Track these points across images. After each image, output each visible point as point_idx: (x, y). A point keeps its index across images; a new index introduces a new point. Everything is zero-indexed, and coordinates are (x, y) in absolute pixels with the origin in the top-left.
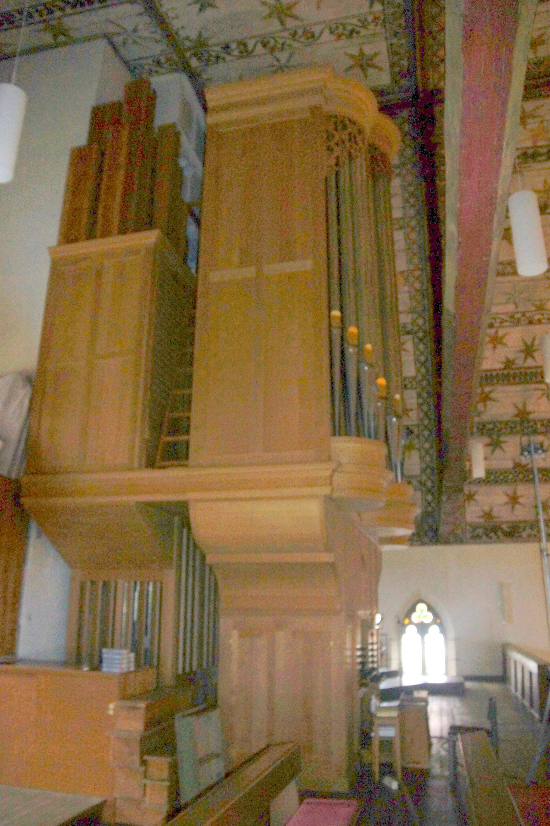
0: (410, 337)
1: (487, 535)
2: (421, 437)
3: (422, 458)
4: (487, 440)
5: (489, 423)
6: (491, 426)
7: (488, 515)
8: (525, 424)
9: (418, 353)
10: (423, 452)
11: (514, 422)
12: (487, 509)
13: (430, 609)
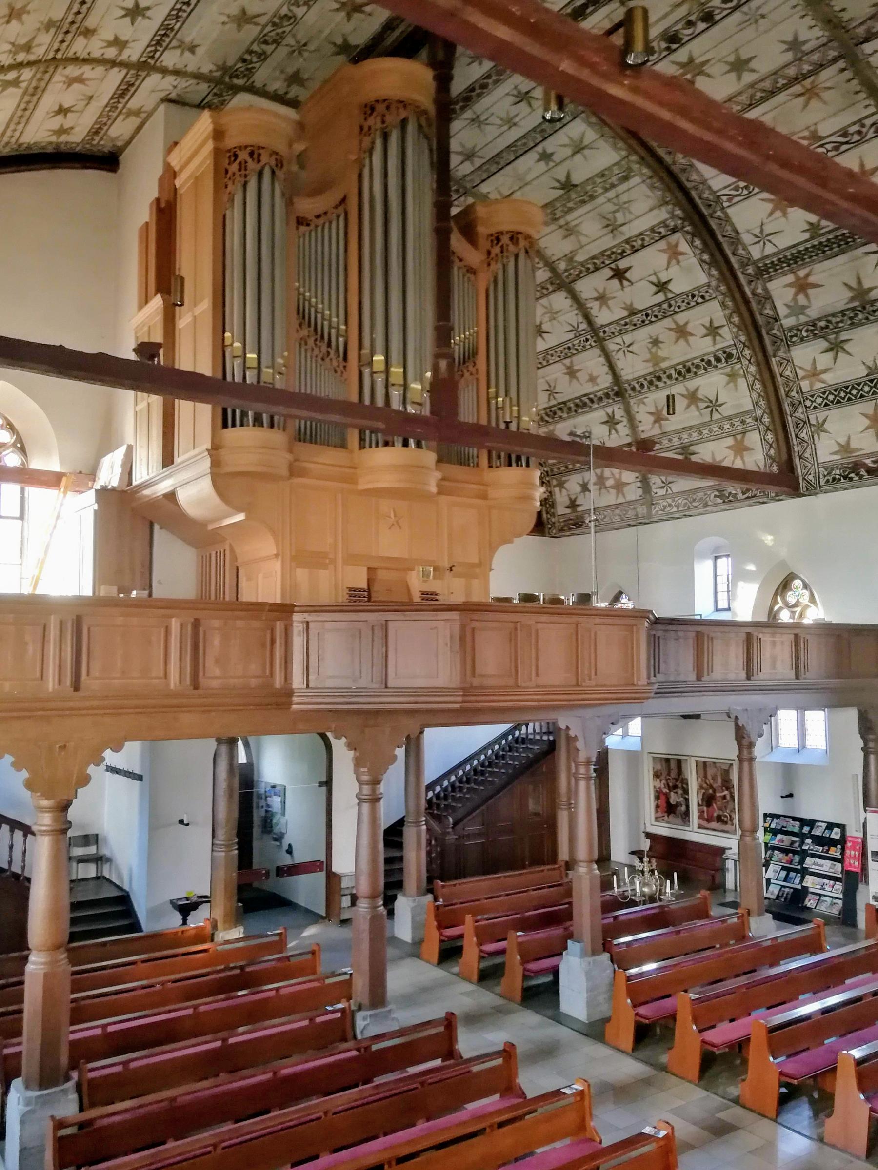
0: (678, 235)
1: (845, 478)
3: (751, 388)
4: (823, 344)
5: (819, 319)
6: (823, 324)
7: (845, 448)
8: (869, 308)
9: (698, 252)
10: (751, 379)
11: (853, 309)
12: (842, 440)
13: (806, 586)
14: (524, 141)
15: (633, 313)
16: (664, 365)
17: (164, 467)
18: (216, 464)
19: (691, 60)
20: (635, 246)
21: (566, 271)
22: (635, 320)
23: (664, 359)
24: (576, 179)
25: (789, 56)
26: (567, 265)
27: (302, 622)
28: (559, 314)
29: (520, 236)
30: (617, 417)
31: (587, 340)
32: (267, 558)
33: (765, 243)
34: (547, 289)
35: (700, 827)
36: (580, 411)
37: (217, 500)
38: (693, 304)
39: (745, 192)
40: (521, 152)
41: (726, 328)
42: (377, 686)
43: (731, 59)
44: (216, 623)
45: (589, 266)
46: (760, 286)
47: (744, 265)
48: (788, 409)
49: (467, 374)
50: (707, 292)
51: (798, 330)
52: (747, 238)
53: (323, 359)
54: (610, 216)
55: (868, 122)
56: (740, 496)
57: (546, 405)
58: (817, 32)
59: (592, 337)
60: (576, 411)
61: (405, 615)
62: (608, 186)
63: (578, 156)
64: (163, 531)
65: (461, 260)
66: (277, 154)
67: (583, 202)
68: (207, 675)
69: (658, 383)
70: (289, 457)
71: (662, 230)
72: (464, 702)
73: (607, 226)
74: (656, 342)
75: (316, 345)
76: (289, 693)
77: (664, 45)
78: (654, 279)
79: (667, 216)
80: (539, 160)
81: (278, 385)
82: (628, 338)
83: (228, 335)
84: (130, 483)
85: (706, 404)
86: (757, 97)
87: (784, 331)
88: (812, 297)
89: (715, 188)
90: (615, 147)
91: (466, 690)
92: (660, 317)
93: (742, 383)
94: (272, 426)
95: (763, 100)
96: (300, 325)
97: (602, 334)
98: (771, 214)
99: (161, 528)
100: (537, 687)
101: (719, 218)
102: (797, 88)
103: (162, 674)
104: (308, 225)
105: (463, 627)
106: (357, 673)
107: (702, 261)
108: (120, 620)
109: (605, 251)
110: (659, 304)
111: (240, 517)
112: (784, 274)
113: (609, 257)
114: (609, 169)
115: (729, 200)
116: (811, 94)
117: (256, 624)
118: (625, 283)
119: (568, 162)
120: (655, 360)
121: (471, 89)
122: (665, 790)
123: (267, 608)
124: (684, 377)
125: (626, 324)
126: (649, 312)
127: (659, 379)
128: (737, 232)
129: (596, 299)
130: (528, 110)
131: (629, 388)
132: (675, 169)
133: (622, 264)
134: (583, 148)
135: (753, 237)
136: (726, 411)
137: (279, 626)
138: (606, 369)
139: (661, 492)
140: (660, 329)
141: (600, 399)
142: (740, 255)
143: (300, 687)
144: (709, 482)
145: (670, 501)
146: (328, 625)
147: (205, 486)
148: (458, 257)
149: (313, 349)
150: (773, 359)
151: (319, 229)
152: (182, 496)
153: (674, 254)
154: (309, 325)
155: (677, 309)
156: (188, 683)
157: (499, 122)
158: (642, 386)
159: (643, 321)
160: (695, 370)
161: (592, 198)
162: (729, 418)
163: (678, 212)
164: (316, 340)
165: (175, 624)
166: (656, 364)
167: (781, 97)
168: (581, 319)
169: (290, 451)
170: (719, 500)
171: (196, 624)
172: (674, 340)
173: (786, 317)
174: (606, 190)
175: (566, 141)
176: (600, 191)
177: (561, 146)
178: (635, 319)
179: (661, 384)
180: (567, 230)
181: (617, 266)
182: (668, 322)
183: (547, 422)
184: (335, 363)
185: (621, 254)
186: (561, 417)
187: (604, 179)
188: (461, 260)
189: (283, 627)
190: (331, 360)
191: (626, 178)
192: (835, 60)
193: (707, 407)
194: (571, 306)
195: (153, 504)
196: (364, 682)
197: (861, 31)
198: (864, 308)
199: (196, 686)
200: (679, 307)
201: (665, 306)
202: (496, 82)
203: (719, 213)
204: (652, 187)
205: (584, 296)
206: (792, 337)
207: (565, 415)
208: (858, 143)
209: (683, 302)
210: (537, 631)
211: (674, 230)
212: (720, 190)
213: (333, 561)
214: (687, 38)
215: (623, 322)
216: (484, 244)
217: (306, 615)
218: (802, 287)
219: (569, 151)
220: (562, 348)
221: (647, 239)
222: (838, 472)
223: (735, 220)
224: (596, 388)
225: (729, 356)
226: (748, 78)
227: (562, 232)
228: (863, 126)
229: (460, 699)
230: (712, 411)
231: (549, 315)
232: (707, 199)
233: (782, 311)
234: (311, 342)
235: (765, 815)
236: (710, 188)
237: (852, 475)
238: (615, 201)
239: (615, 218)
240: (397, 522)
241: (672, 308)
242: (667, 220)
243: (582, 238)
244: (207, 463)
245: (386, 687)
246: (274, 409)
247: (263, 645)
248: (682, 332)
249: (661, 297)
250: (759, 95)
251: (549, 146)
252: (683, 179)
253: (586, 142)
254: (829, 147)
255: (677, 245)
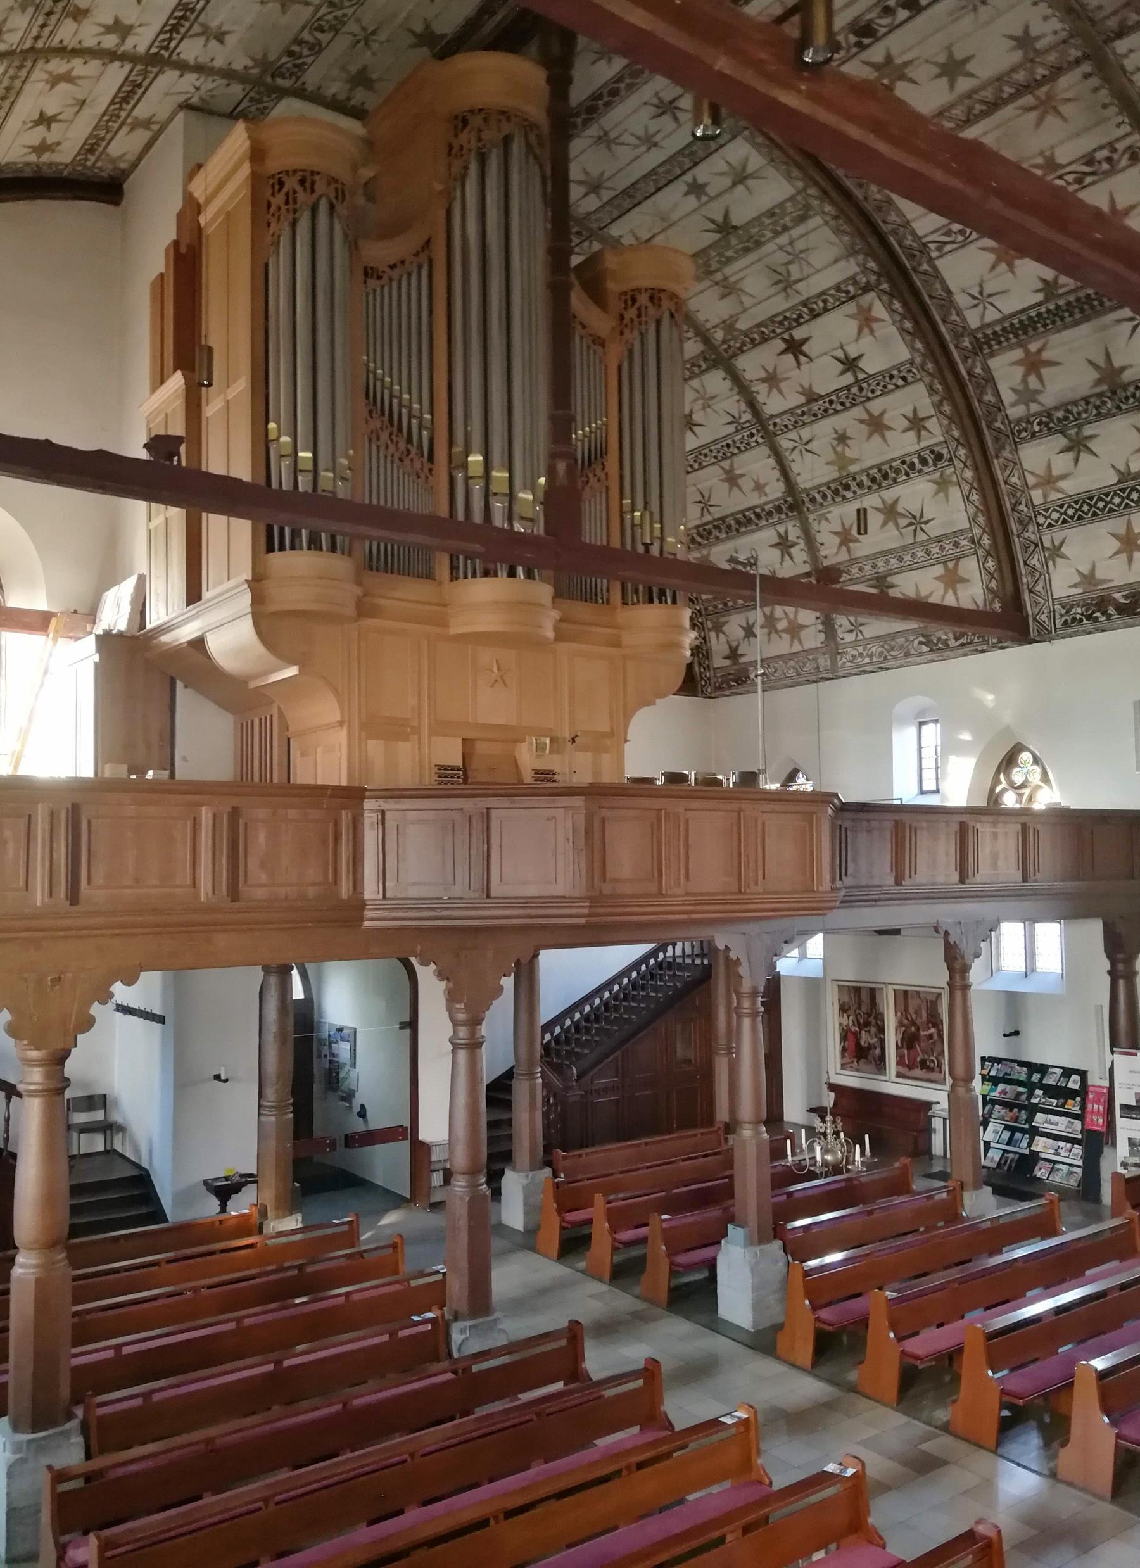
0: (872, 294)
1: (1089, 617)
2: (956, 462)
3: (967, 499)
4: (1060, 441)
5: (1056, 408)
7: (1089, 579)
8: (1121, 394)
9: (898, 318)
10: (966, 488)
11: (1100, 395)
12: (1085, 570)
13: (1036, 760)
14: (668, 166)
15: (812, 397)
16: (853, 469)
17: (188, 604)
18: (258, 600)
19: (889, 59)
20: (815, 309)
21: (724, 342)
22: (816, 408)
23: (854, 461)
24: (737, 219)
25: (1017, 56)
26: (725, 335)
27: (377, 811)
28: (715, 401)
29: (663, 295)
30: (792, 537)
31: (752, 435)
32: (330, 726)
33: (985, 308)
34: (700, 366)
35: (899, 1075)
36: (743, 529)
37: (261, 649)
38: (890, 387)
39: (960, 238)
40: (663, 182)
41: (934, 419)
42: (477, 895)
43: (942, 58)
44: (262, 813)
45: (756, 336)
46: (978, 364)
47: (957, 336)
48: (1014, 527)
49: (593, 481)
50: (909, 371)
51: (1028, 422)
52: (961, 300)
53: (401, 460)
54: (782, 270)
55: (1121, 146)
56: (952, 643)
57: (698, 522)
58: (1055, 24)
59: (758, 431)
60: (737, 530)
61: (512, 802)
62: (779, 229)
63: (740, 188)
64: (189, 690)
65: (584, 327)
66: (336, 181)
67: (747, 250)
68: (249, 883)
69: (845, 493)
70: (358, 591)
71: (851, 288)
72: (589, 915)
73: (777, 283)
74: (842, 438)
75: (392, 440)
76: (362, 905)
77: (853, 39)
78: (840, 354)
79: (858, 270)
80: (687, 194)
81: (341, 496)
82: (805, 433)
83: (272, 425)
84: (143, 625)
85: (907, 521)
86: (976, 112)
87: (1010, 423)
88: (1045, 378)
89: (920, 233)
90: (789, 177)
91: (594, 900)
92: (848, 405)
93: (955, 493)
94: (333, 549)
95: (984, 114)
96: (370, 412)
97: (771, 428)
98: (993, 268)
99: (186, 687)
100: (687, 894)
101: (925, 273)
102: (1028, 100)
103: (189, 881)
104: (379, 278)
105: (589, 818)
106: (451, 878)
107: (902, 330)
108: (131, 810)
109: (776, 316)
110: (848, 388)
111: (292, 671)
112: (1011, 348)
113: (781, 323)
114: (781, 205)
115: (939, 249)
116: (1048, 107)
117: (315, 814)
118: (802, 359)
119: (727, 196)
120: (842, 462)
121: (596, 96)
122: (855, 1029)
123: (329, 792)
124: (880, 485)
125: (803, 413)
126: (834, 397)
127: (847, 487)
128: (949, 292)
129: (763, 380)
130: (674, 125)
131: (806, 499)
132: (869, 207)
133: (798, 334)
134: (745, 178)
135: (969, 298)
136: (934, 529)
137: (345, 817)
138: (777, 474)
139: (849, 638)
140: (848, 420)
141: (770, 514)
142: (954, 323)
143: (373, 897)
144: (912, 625)
145: (860, 649)
146: (411, 815)
147: (245, 629)
148: (581, 323)
149: (387, 447)
150: (996, 461)
151: (395, 285)
152: (214, 645)
153: (866, 321)
154: (383, 414)
155: (870, 395)
156: (225, 893)
157: (636, 142)
158: (824, 497)
159: (826, 411)
160: (894, 475)
161: (758, 244)
162: (939, 539)
163: (872, 264)
164: (391, 434)
165: (206, 815)
166: (840, 469)
167: (1008, 111)
168: (743, 407)
169: (359, 583)
170: (925, 649)
171: (235, 814)
172: (866, 435)
173: (1013, 405)
174: (777, 234)
175: (723, 167)
176: (769, 235)
177: (716, 174)
178: (815, 407)
179: (849, 495)
180: (725, 287)
181: (791, 335)
182: (858, 412)
183: (700, 544)
184: (417, 465)
185: (796, 320)
186: (717, 538)
187: (774, 219)
188: (584, 327)
189: (350, 818)
190: (412, 460)
191: (803, 219)
192: (1078, 62)
193: (911, 524)
194: (731, 390)
195: (176, 653)
196: (458, 891)
197: (1113, 23)
198: (1114, 393)
199: (234, 894)
200: (873, 391)
201: (855, 390)
202: (630, 87)
203: (925, 267)
204: (837, 231)
205: (748, 376)
206: (1020, 432)
207: (723, 536)
208: (1107, 174)
209: (878, 384)
210: (687, 821)
211: (866, 289)
212: (925, 236)
213: (417, 730)
214: (883, 30)
215: (799, 412)
216: (615, 305)
217: (381, 801)
218: (1034, 365)
219: (727, 181)
220: (718, 446)
221: (831, 300)
222: (1079, 610)
223: (946, 275)
224: (764, 499)
225: (939, 457)
226: (964, 84)
227: (718, 290)
228: (1114, 150)
229: (586, 911)
230: (915, 531)
231: (700, 402)
232: (911, 247)
233: (1008, 397)
234: (385, 436)
235: (983, 1059)
236: (913, 233)
237: (1098, 614)
238: (789, 249)
239: (788, 272)
240: (502, 677)
241: (864, 393)
242: (856, 274)
243: (745, 299)
244: (247, 598)
245: (488, 896)
246: (334, 527)
247: (325, 842)
248: (876, 425)
249: (849, 378)
250: (978, 107)
251: (702, 173)
252: (877, 218)
253: (750, 169)
254: (1070, 178)
255: (870, 309)
